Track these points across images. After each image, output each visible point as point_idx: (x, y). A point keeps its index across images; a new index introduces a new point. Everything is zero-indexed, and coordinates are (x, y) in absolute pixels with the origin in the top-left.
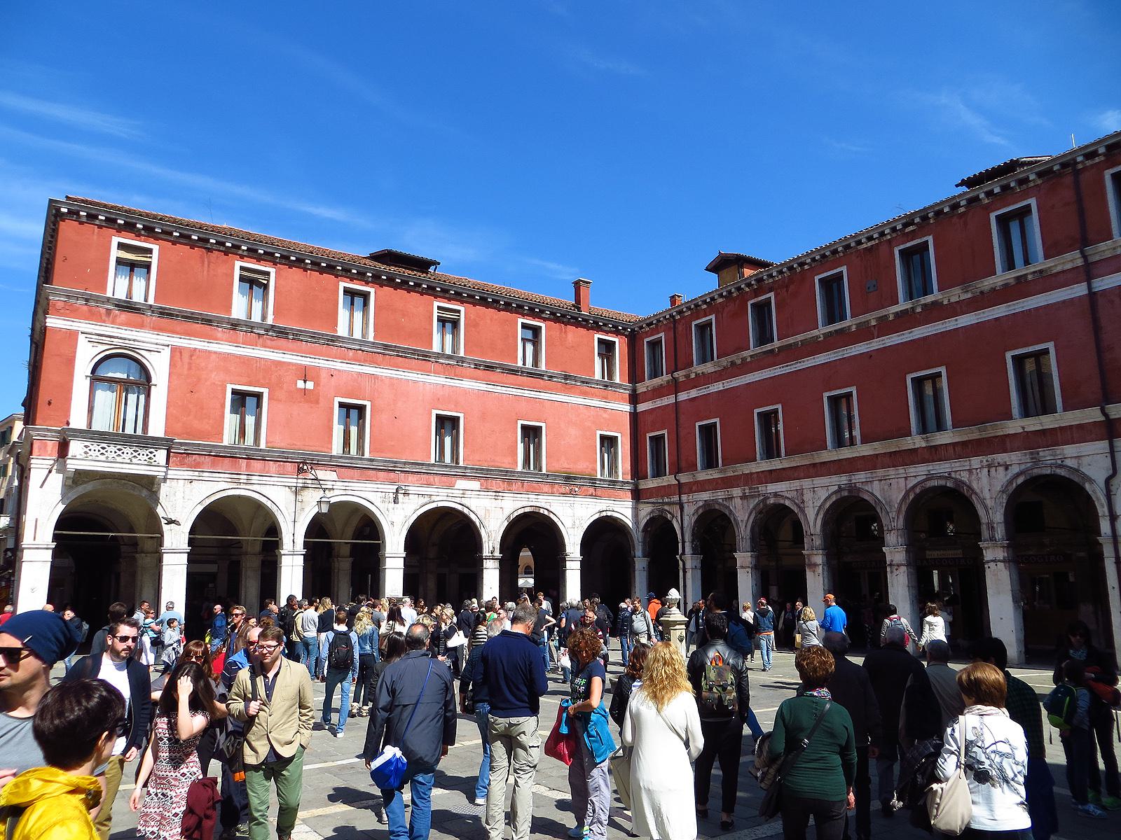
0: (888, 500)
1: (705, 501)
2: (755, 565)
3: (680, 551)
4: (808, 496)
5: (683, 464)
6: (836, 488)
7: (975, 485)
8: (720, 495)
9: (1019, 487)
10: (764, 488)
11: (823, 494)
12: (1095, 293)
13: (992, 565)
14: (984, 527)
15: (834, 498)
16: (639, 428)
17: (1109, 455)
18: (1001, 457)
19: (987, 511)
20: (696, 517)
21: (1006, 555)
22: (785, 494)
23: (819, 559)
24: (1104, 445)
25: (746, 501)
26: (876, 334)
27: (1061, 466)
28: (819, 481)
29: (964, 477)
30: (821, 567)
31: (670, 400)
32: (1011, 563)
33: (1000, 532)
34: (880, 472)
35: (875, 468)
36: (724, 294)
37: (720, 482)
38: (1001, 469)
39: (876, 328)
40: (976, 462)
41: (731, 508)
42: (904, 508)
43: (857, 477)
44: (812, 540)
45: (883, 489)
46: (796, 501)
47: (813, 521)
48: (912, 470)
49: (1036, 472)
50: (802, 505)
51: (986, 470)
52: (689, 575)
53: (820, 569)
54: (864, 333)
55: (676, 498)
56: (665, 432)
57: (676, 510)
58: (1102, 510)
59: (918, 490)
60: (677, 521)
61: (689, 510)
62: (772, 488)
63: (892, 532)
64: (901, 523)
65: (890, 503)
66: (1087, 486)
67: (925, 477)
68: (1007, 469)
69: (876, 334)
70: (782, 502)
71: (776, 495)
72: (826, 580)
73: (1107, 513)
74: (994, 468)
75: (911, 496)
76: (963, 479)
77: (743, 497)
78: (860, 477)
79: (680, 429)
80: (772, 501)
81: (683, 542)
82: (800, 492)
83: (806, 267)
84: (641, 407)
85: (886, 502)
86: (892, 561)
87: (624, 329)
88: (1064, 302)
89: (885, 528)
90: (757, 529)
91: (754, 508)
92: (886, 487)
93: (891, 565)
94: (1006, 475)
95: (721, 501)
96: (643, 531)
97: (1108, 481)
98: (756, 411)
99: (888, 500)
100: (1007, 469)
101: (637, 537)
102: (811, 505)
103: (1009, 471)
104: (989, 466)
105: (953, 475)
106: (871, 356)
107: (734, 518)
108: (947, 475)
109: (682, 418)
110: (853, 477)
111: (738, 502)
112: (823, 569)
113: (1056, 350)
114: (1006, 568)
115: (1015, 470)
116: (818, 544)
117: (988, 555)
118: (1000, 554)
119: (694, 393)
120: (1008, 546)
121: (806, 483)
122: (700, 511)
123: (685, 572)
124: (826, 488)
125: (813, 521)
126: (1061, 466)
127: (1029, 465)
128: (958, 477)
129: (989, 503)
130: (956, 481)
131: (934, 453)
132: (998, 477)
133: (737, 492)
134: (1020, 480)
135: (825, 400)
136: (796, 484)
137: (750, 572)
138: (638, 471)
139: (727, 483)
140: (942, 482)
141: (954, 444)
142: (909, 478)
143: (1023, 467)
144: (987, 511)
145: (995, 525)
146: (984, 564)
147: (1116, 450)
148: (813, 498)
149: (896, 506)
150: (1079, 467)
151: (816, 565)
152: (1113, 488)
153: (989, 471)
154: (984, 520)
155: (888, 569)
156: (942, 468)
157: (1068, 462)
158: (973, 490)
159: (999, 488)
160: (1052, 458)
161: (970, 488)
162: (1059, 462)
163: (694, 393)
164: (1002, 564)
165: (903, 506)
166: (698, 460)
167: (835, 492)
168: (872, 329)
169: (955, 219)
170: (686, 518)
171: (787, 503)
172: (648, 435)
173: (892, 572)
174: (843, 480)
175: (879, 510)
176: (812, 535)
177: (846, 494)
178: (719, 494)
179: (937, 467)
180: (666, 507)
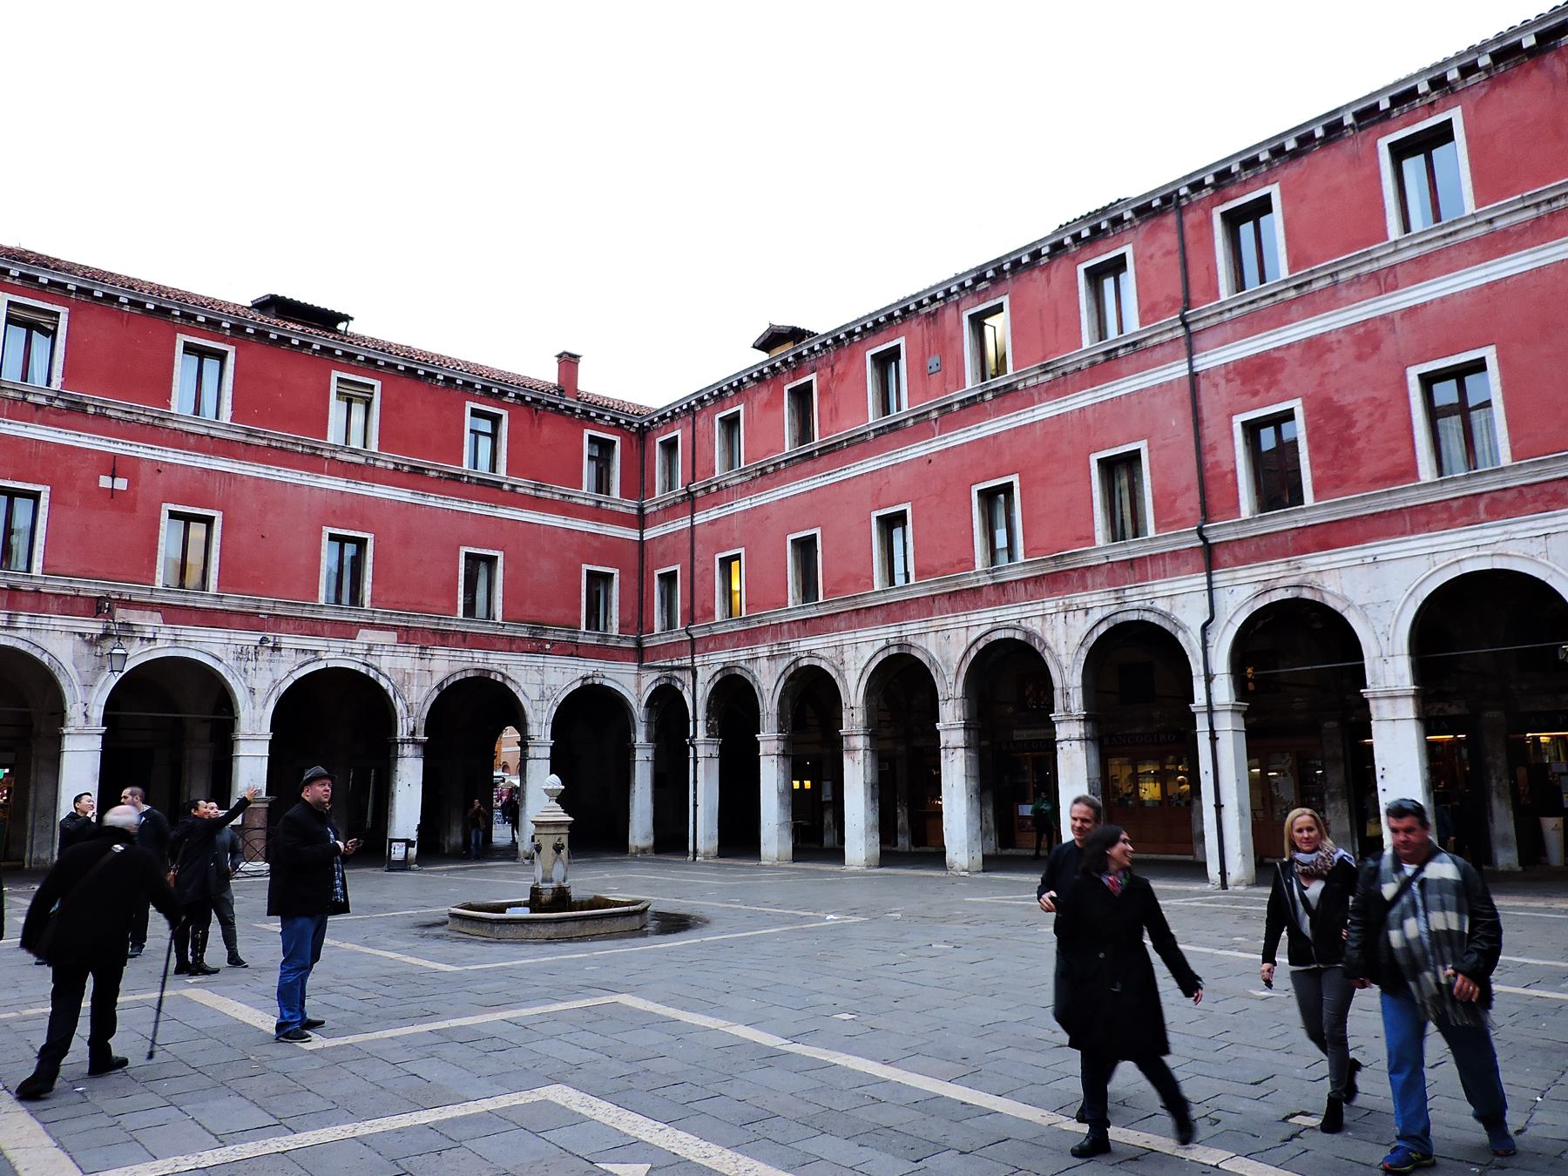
0: (945, 659)
1: (724, 663)
2: (784, 751)
3: (691, 734)
4: (849, 654)
5: (698, 612)
6: (883, 643)
7: (1048, 638)
8: (743, 654)
9: (1101, 638)
10: (796, 644)
11: (868, 652)
12: (1197, 374)
13: (1065, 744)
14: (1057, 694)
15: (880, 658)
16: (645, 564)
17: (1206, 593)
18: (1081, 599)
19: (1061, 671)
20: (712, 685)
21: (1083, 731)
22: (822, 653)
23: (859, 742)
24: (1202, 579)
25: (773, 662)
26: (937, 431)
27: (1149, 610)
28: (863, 634)
29: (1035, 626)
30: (862, 751)
31: (683, 523)
32: (1089, 742)
33: (1077, 702)
34: (937, 622)
35: (931, 614)
36: (755, 375)
37: (742, 635)
38: (1080, 614)
39: (938, 423)
40: (1050, 605)
41: (755, 672)
42: (964, 669)
43: (909, 627)
44: (852, 715)
45: (940, 643)
46: (835, 662)
47: (853, 692)
48: (975, 617)
49: (1121, 618)
50: (841, 668)
51: (1062, 615)
52: (701, 766)
53: (860, 755)
54: (921, 425)
55: (687, 662)
56: (677, 567)
57: (687, 677)
58: (1197, 669)
59: (981, 645)
60: (689, 691)
61: (704, 675)
62: (807, 644)
63: (949, 702)
64: (959, 690)
65: (946, 662)
66: (1181, 637)
67: (989, 627)
68: (1087, 614)
69: (937, 431)
70: (817, 663)
71: (810, 654)
72: (869, 770)
73: (1202, 672)
74: (1072, 613)
75: (973, 653)
76: (1034, 628)
77: (771, 657)
78: (911, 628)
79: (696, 563)
80: (804, 663)
81: (695, 721)
82: (839, 648)
83: (856, 338)
84: (649, 534)
85: (943, 661)
86: (947, 742)
87: (628, 423)
88: (1161, 385)
89: (940, 698)
90: (787, 702)
91: (783, 673)
92: (943, 641)
93: (945, 748)
94: (1086, 622)
95: (743, 663)
96: (647, 705)
97: (1204, 628)
98: (791, 537)
99: (945, 659)
100: (1087, 614)
101: (639, 712)
102: (853, 667)
103: (1089, 616)
106: (930, 461)
107: (759, 688)
108: (1015, 623)
109: (698, 547)
110: (904, 628)
111: (763, 663)
112: (865, 755)
113: (1150, 451)
114: (1082, 749)
115: (1097, 615)
116: (859, 720)
117: (1062, 731)
118: (1077, 729)
119: (715, 514)
120: (1086, 720)
121: (847, 637)
122: (718, 677)
123: (696, 762)
124: (871, 643)
125: (853, 692)
126: (1149, 610)
127: (1113, 609)
128: (1029, 625)
129: (1065, 661)
130: (1026, 632)
131: (1002, 592)
132: (1076, 624)
133: (763, 650)
134: (1103, 629)
135: (874, 521)
136: (835, 639)
137: (776, 760)
138: (642, 623)
139: (751, 637)
140: (1009, 634)
141: (1025, 581)
142: (970, 628)
143: (1106, 612)
144: (1061, 671)
145: (1071, 691)
146: (1056, 743)
147: (1214, 586)
148: (856, 657)
149: (955, 667)
150: (1171, 609)
151: (855, 750)
152: (1210, 638)
153: (1066, 617)
154: (1057, 684)
155: (943, 753)
156: (1008, 614)
157: (1161, 605)
158: (1045, 644)
159: (1078, 640)
160: (1140, 597)
161: (1042, 641)
162: (1148, 604)
163: (715, 514)
164: (1078, 742)
165: (963, 665)
166: (717, 606)
167: (883, 649)
168: (933, 422)
169: (1036, 273)
170: (699, 687)
171: (824, 665)
172: (657, 572)
173: (946, 757)
174: (890, 632)
175: (933, 673)
176: (852, 708)
177: (894, 651)
178: (741, 653)
179: (1004, 612)
180: (676, 673)
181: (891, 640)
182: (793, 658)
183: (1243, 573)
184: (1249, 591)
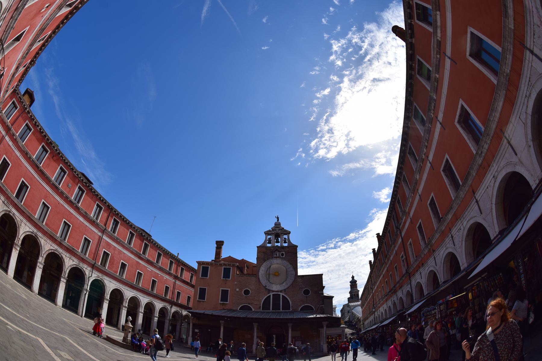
11: (28, 229)
22: (17, 217)
29: (64, 256)
46: (19, 223)
48: (53, 245)
49: (78, 267)
59: (52, 251)
67: (55, 249)
71: (14, 214)
104: (70, 258)
105: (62, 254)
108: (61, 253)
115: (75, 263)
143: (76, 264)
157: (84, 269)
161: (64, 260)
162: (83, 267)
174: (35, 231)
181: (34, 232)
182: (9, 210)
183: (96, 273)
184: (96, 275)
